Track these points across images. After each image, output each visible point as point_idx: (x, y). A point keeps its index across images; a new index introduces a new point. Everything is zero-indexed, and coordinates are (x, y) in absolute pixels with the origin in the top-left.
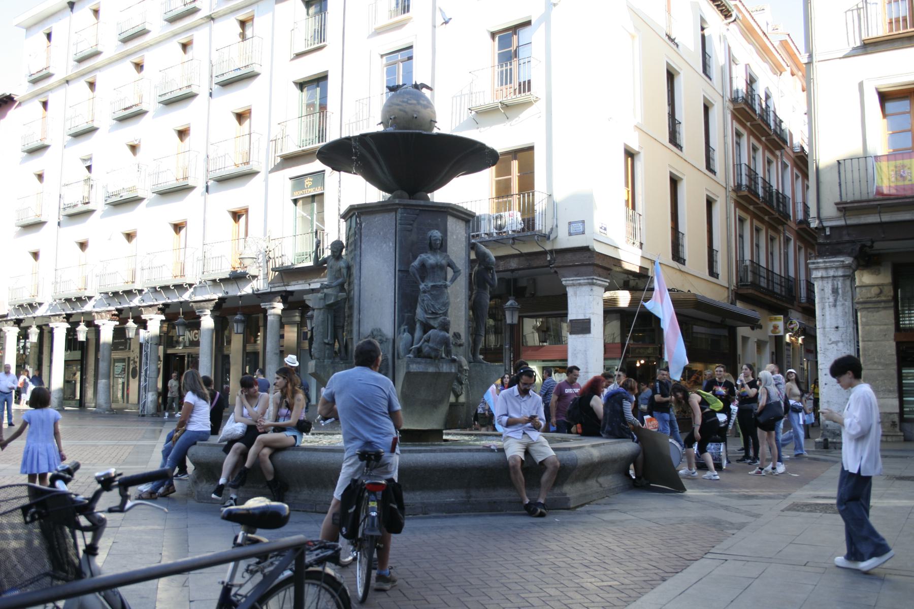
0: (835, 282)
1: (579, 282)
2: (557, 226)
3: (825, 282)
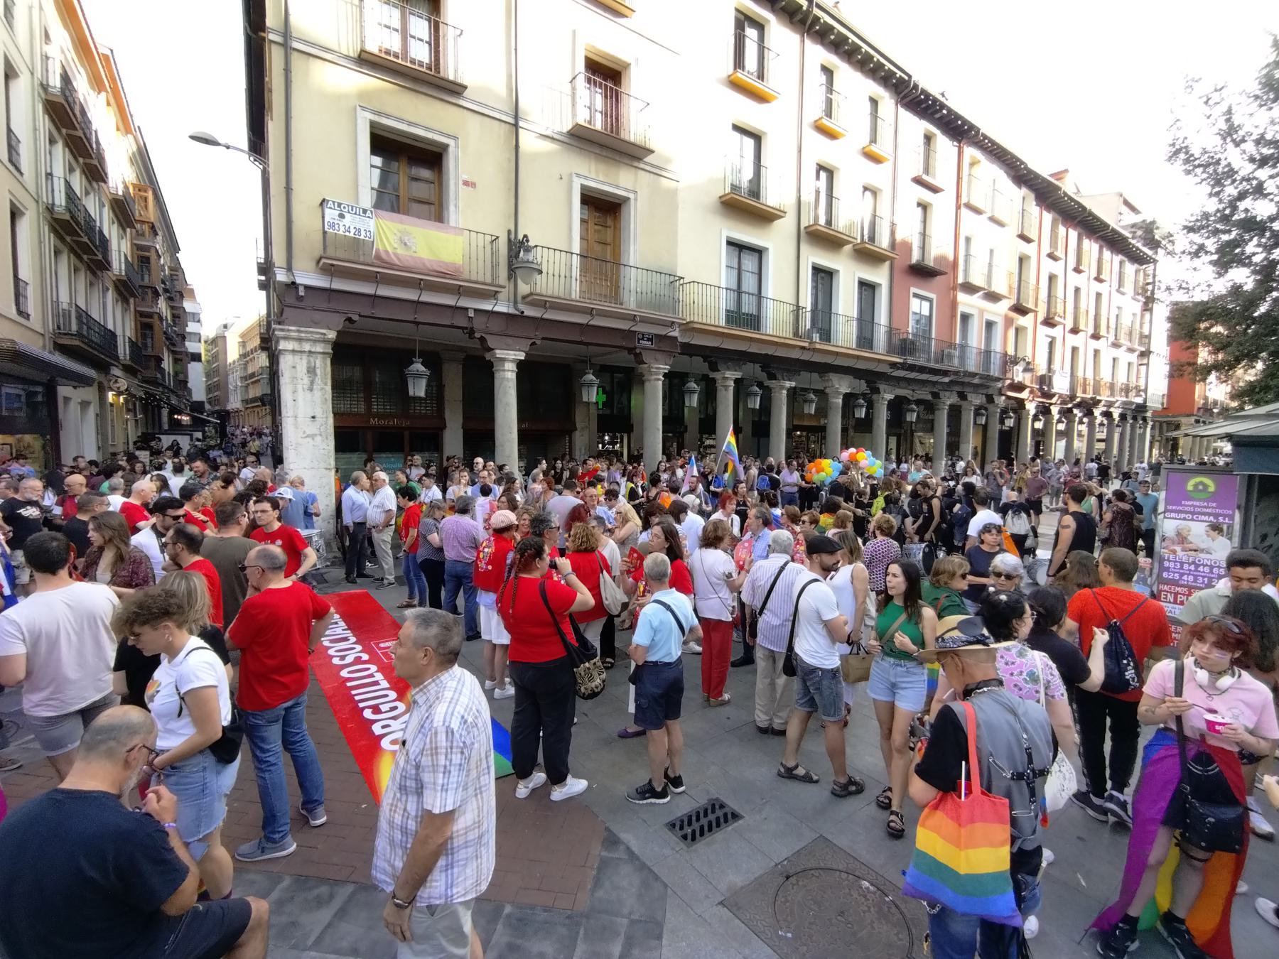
0: (312, 359)
3: (297, 357)
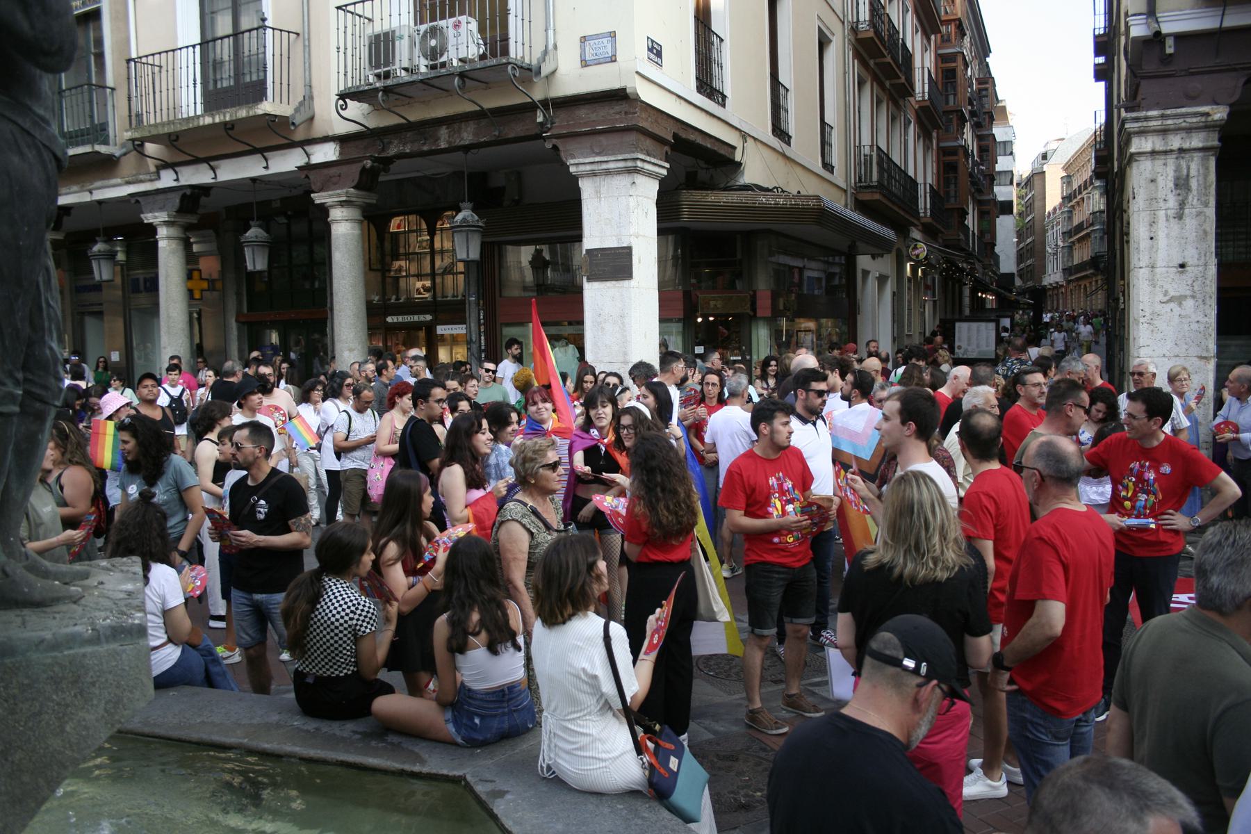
0: (1183, 164)
1: (604, 166)
2: (555, 47)
3: (1159, 162)
